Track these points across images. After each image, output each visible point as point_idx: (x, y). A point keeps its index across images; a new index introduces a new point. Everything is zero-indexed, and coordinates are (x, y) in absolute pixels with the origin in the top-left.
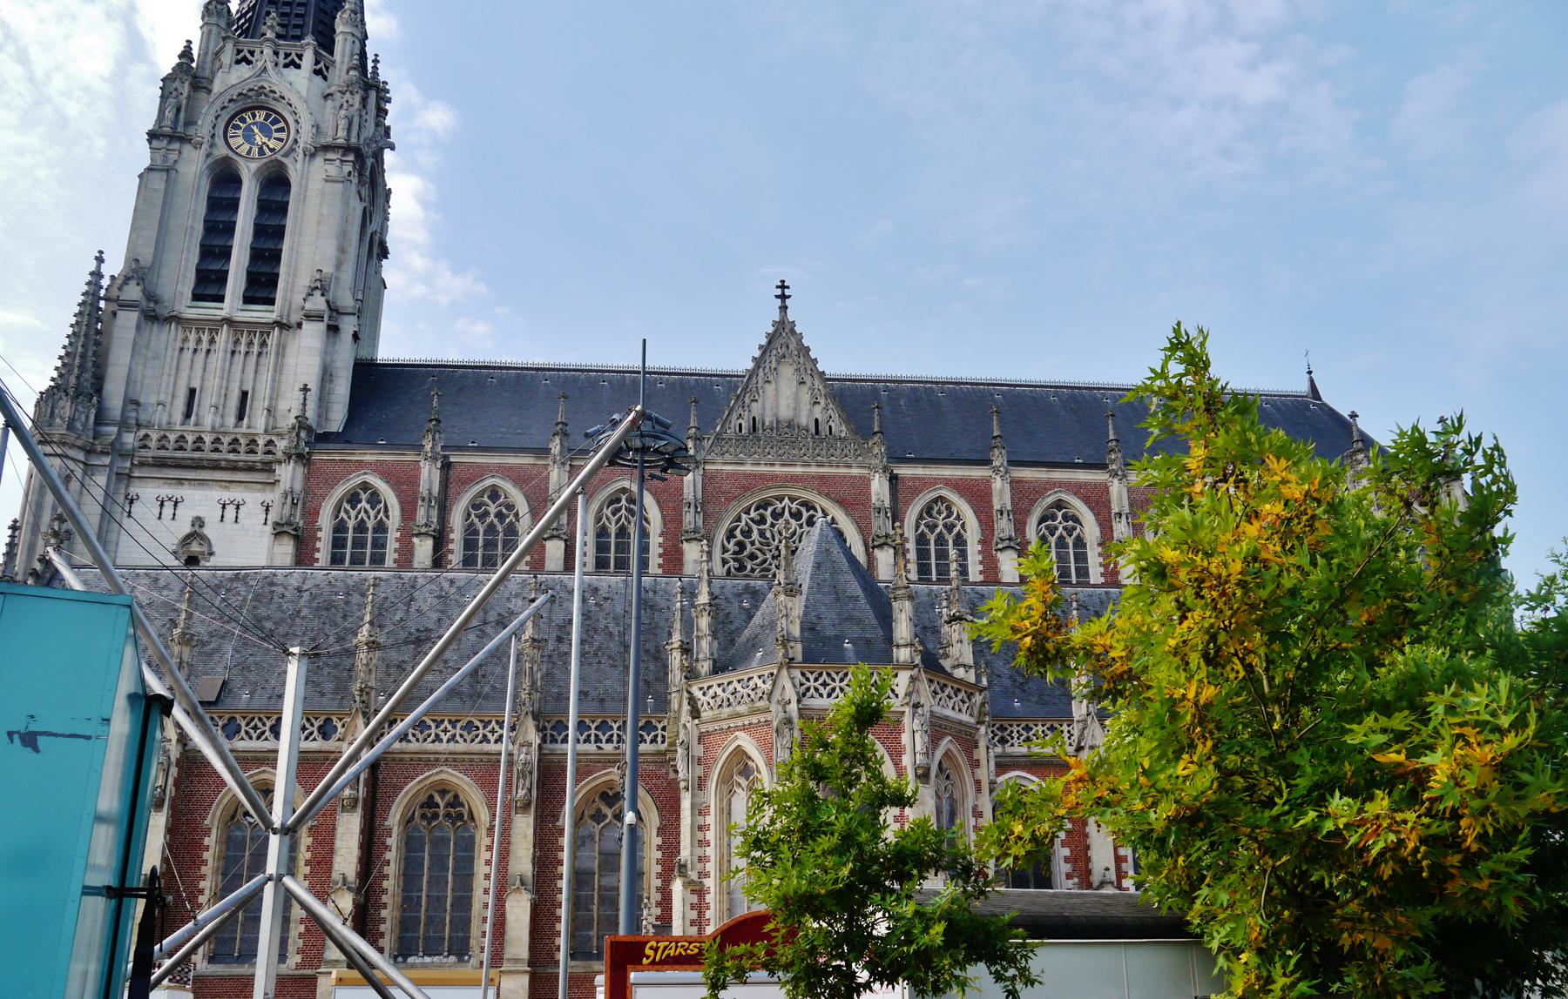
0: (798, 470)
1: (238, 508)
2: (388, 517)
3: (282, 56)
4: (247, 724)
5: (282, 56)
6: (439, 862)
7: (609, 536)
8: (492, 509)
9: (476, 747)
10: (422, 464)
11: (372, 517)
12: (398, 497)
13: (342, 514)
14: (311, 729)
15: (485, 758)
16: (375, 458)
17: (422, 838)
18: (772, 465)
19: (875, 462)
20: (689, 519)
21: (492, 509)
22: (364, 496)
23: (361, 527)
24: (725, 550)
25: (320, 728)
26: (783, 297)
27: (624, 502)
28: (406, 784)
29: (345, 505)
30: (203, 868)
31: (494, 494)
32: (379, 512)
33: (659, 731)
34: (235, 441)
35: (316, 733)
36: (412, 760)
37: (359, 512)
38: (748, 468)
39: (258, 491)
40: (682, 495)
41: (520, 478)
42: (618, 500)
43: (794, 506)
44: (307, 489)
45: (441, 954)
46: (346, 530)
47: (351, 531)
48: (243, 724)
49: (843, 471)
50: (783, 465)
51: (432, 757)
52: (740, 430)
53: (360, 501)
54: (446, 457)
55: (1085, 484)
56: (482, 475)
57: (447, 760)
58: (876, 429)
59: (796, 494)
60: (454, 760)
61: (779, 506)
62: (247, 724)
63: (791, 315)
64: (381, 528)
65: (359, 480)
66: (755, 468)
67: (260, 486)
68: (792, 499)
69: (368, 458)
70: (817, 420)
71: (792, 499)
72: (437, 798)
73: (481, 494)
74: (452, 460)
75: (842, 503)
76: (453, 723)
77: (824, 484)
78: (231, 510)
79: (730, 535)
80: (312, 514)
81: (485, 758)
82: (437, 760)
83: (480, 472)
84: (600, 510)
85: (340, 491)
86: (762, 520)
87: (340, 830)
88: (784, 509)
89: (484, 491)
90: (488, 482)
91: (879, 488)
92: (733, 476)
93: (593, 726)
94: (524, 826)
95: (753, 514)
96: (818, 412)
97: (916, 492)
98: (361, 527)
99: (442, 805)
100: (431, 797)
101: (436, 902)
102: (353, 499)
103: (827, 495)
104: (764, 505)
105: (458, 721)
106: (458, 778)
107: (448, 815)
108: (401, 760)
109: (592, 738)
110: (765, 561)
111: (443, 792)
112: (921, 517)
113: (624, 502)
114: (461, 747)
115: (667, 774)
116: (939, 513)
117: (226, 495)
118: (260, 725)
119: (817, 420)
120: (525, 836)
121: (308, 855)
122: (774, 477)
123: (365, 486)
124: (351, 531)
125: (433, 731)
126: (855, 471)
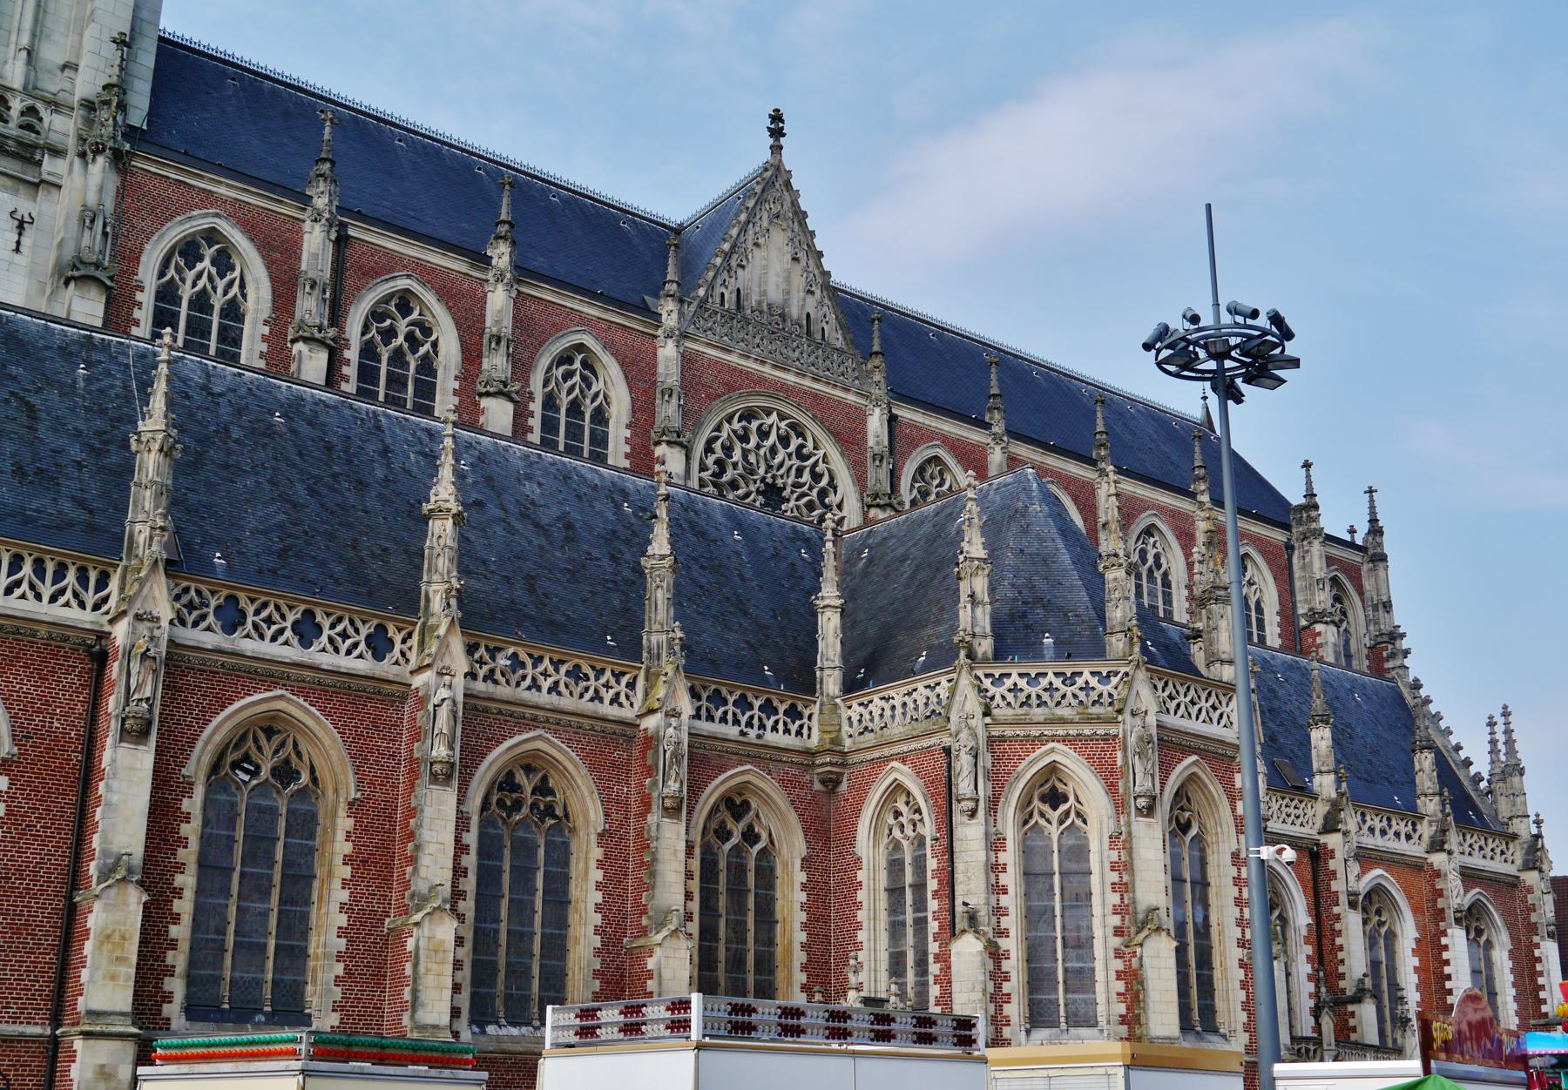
0: (791, 378)
2: (244, 296)
4: (257, 612)
6: (523, 876)
7: (558, 410)
8: (402, 326)
9: (585, 705)
10: (307, 226)
11: (220, 290)
12: (268, 268)
13: (171, 272)
14: (357, 638)
15: (599, 725)
16: (233, 194)
17: (500, 837)
18: (763, 363)
19: (876, 392)
20: (668, 412)
21: (402, 326)
22: (209, 253)
23: (201, 302)
24: (703, 468)
25: (368, 637)
26: (776, 133)
27: (577, 365)
28: (490, 749)
29: (177, 258)
30: (181, 851)
31: (405, 302)
32: (230, 284)
33: (805, 720)
35: (362, 646)
36: (500, 712)
37: (199, 276)
38: (733, 359)
40: (654, 374)
41: (448, 292)
42: (570, 361)
43: (783, 425)
44: (120, 214)
45: (529, 1024)
46: (177, 301)
47: (185, 303)
48: (251, 609)
49: (839, 393)
50: (775, 367)
51: (528, 712)
52: (722, 303)
53: (201, 259)
54: (343, 226)
55: (1075, 479)
56: (392, 270)
57: (547, 721)
58: (876, 348)
59: (787, 410)
60: (557, 721)
61: (769, 421)
62: (257, 612)
64: (233, 312)
65: (205, 223)
66: (742, 362)
67: (9, 183)
68: (782, 417)
69: (222, 190)
70: (808, 315)
71: (782, 417)
72: (521, 777)
73: (387, 299)
74: (351, 232)
75: (837, 436)
76: (557, 664)
77: (816, 403)
79: (709, 449)
80: (132, 259)
81: (599, 725)
82: (535, 719)
83: (388, 265)
84: (549, 369)
85: (174, 232)
86: (744, 438)
87: (428, 812)
88: (771, 426)
89: (391, 296)
90: (403, 283)
91: (876, 424)
92: (716, 363)
93: (731, 700)
94: (673, 836)
95: (736, 425)
96: (811, 305)
97: (914, 444)
98: (201, 302)
99: (528, 789)
100: (510, 774)
101: (519, 939)
102: (189, 251)
103: (823, 424)
104: (748, 415)
105: (563, 662)
106: (560, 750)
107: (534, 806)
108: (486, 710)
109: (730, 717)
110: (747, 495)
111: (528, 769)
112: (914, 480)
113: (577, 365)
114: (567, 702)
115: (811, 782)
116: (932, 478)
118: (276, 616)
119: (808, 315)
120: (675, 853)
121: (348, 848)
122: (761, 380)
123: (212, 235)
124: (185, 303)
125: (529, 671)
126: (851, 398)
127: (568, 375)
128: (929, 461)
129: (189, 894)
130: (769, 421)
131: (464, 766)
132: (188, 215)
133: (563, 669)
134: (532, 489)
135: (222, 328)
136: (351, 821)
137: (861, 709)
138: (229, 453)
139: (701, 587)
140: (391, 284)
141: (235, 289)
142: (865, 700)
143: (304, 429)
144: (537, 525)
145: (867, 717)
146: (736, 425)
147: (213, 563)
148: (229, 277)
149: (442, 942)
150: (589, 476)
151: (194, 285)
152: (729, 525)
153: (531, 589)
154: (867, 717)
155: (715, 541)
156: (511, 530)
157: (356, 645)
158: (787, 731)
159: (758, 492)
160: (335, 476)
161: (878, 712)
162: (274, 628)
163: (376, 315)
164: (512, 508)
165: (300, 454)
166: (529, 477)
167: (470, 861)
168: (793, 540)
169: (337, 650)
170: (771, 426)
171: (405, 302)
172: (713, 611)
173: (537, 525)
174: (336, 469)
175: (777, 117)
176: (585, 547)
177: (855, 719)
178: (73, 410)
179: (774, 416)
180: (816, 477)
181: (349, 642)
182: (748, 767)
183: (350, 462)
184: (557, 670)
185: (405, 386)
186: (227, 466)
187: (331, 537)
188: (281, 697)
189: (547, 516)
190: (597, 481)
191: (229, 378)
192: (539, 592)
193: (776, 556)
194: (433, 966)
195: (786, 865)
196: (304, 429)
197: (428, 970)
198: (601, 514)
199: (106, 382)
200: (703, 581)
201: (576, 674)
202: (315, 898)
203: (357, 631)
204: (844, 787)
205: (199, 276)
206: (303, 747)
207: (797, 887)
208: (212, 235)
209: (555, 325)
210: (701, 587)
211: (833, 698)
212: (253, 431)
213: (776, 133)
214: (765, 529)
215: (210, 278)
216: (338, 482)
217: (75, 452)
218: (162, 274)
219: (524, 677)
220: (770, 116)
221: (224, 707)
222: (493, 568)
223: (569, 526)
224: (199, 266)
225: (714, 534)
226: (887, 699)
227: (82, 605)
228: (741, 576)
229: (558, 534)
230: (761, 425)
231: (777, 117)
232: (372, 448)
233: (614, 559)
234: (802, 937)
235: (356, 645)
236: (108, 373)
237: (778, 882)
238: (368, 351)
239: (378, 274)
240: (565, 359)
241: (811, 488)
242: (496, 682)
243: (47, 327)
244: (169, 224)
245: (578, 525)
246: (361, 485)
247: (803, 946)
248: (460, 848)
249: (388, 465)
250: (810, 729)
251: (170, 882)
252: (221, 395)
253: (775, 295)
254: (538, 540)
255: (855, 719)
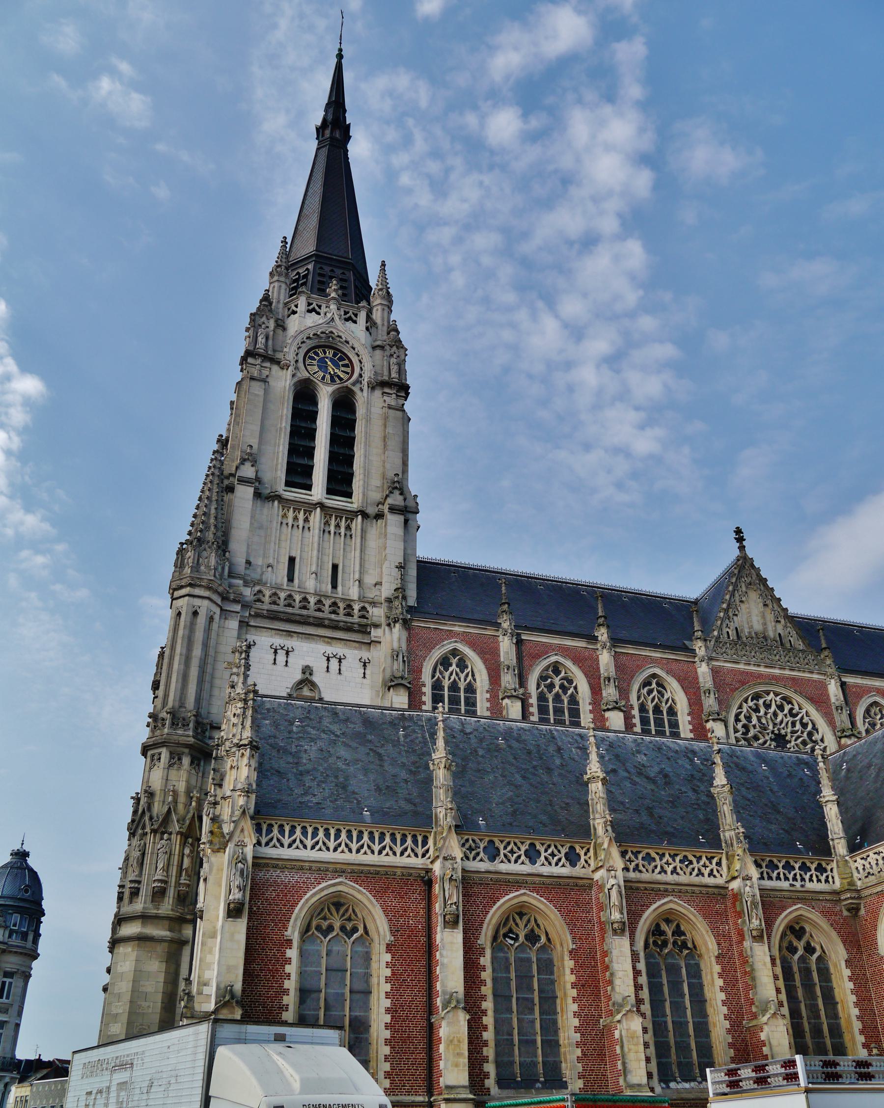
0: (777, 671)
1: (340, 662)
2: (475, 680)
4: (505, 848)
6: (675, 987)
7: (647, 712)
8: (557, 681)
9: (694, 879)
10: (501, 638)
11: (462, 679)
12: (485, 663)
13: (438, 674)
14: (560, 856)
15: (704, 890)
16: (462, 629)
17: (658, 964)
18: (759, 666)
19: (829, 670)
20: (710, 703)
21: (557, 681)
22: (454, 661)
23: (454, 687)
24: (736, 731)
25: (566, 854)
26: (740, 539)
27: (654, 685)
28: (643, 911)
29: (439, 667)
30: (483, 988)
31: (556, 668)
32: (467, 675)
33: (829, 873)
34: (334, 604)
35: (563, 860)
36: (646, 889)
37: (451, 674)
38: (741, 666)
39: (355, 648)
40: (698, 683)
41: (578, 659)
42: (650, 684)
43: (778, 698)
44: (410, 651)
45: (694, 1080)
46: (442, 688)
47: (446, 689)
48: (501, 847)
50: (766, 667)
51: (662, 887)
52: (729, 637)
53: (451, 665)
54: (519, 635)
56: (547, 653)
57: (673, 891)
58: (824, 646)
59: (778, 690)
60: (679, 890)
61: (769, 698)
62: (505, 848)
63: (750, 553)
64: (470, 689)
65: (450, 647)
67: (357, 645)
68: (776, 694)
69: (456, 629)
70: (780, 634)
72: (664, 927)
73: (547, 669)
74: (523, 637)
75: (812, 700)
76: (673, 857)
77: (795, 683)
78: (334, 663)
79: (737, 720)
80: (416, 671)
81: (704, 890)
82: (666, 890)
83: (546, 650)
84: (639, 690)
85: (437, 654)
86: (757, 710)
87: (615, 953)
88: (771, 701)
89: (549, 666)
90: (554, 659)
91: (833, 689)
92: (732, 670)
93: (780, 865)
94: (761, 954)
95: (751, 704)
96: (780, 628)
97: (859, 696)
98: (454, 687)
99: (670, 933)
100: (658, 925)
101: (680, 1026)
102: (445, 662)
103: (801, 694)
104: (756, 697)
105: (677, 855)
106: (684, 908)
107: (675, 943)
108: (637, 889)
109: (782, 876)
110: (765, 742)
111: (668, 921)
112: (864, 718)
113: (654, 685)
114: (683, 879)
115: (841, 911)
116: (876, 714)
117: (330, 650)
118: (515, 849)
119: (780, 634)
120: (765, 964)
121: (573, 978)
122: (760, 676)
123: (455, 652)
124: (446, 689)
125: (658, 862)
126: (815, 676)
127: (650, 692)
128: (871, 705)
129: (490, 1013)
130: (769, 698)
131: (631, 923)
132: (442, 644)
133: (640, 856)
134: (641, 758)
135: (466, 698)
136: (572, 962)
137: (863, 862)
138: (479, 763)
139: (749, 800)
140: (548, 660)
141: (470, 677)
142: (864, 856)
143: (515, 744)
144: (648, 778)
145: (868, 866)
146: (751, 704)
147: (479, 824)
148: (466, 672)
149: (635, 1032)
150: (672, 745)
151: (449, 679)
152: (758, 761)
153: (651, 815)
154: (868, 866)
155: (751, 772)
156: (635, 783)
157: (560, 860)
158: (819, 881)
159: (771, 740)
160: (534, 767)
161: (873, 863)
162: (515, 855)
163: (543, 678)
164: (633, 771)
165: (515, 758)
166: (639, 752)
167: (643, 980)
168: (798, 765)
169: (550, 864)
170: (771, 701)
171: (556, 668)
172: (759, 813)
173: (648, 778)
174: (534, 763)
175: (738, 531)
176: (677, 787)
177: (861, 868)
178: (400, 753)
179: (772, 695)
180: (804, 726)
181: (556, 858)
182: (799, 906)
183: (541, 758)
184: (674, 860)
185: (564, 712)
186: (479, 771)
187: (538, 801)
188: (524, 894)
189: (652, 772)
190: (677, 748)
191: (473, 724)
192: (656, 816)
193: (790, 775)
194: (632, 1047)
195: (835, 966)
196: (515, 744)
197: (630, 1050)
198: (682, 766)
199: (414, 736)
200: (750, 796)
201: (648, 858)
202: (559, 1010)
203: (559, 851)
204: (862, 912)
205: (451, 674)
206: (539, 922)
207: (846, 979)
208: (455, 652)
209: (638, 666)
210: (749, 800)
211: (844, 857)
212: (489, 750)
213: (740, 539)
214: (780, 760)
215: (457, 674)
216: (537, 770)
217: (403, 774)
218: (433, 676)
219: (656, 867)
220: (735, 531)
221: (495, 903)
222: (627, 806)
223: (666, 776)
224: (451, 669)
225: (750, 768)
226: (878, 853)
227: (416, 855)
228: (771, 790)
229: (660, 781)
230: (765, 701)
231: (738, 531)
232: (551, 749)
233: (694, 790)
234: (855, 1012)
235: (560, 860)
236: (414, 731)
237: (833, 977)
238: (542, 698)
239: (540, 656)
240: (647, 683)
241: (802, 733)
242: (640, 871)
243: (382, 712)
244: (433, 651)
245: (671, 774)
246: (549, 770)
247: (858, 1017)
248: (637, 973)
249: (562, 757)
250: (833, 878)
251: (479, 1007)
252: (470, 733)
253: (758, 627)
254: (650, 786)
255: (861, 868)
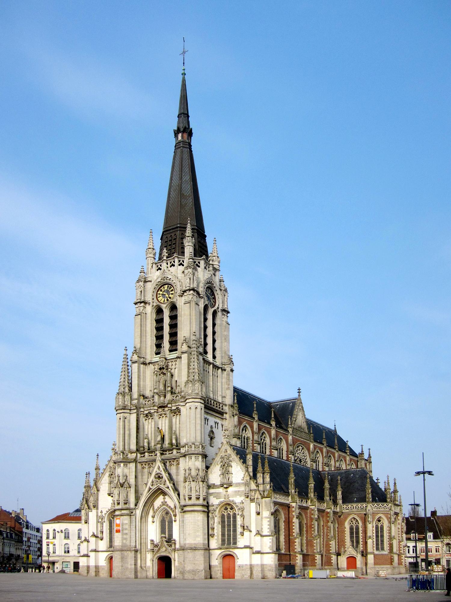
3: (169, 263)
5: (169, 263)
